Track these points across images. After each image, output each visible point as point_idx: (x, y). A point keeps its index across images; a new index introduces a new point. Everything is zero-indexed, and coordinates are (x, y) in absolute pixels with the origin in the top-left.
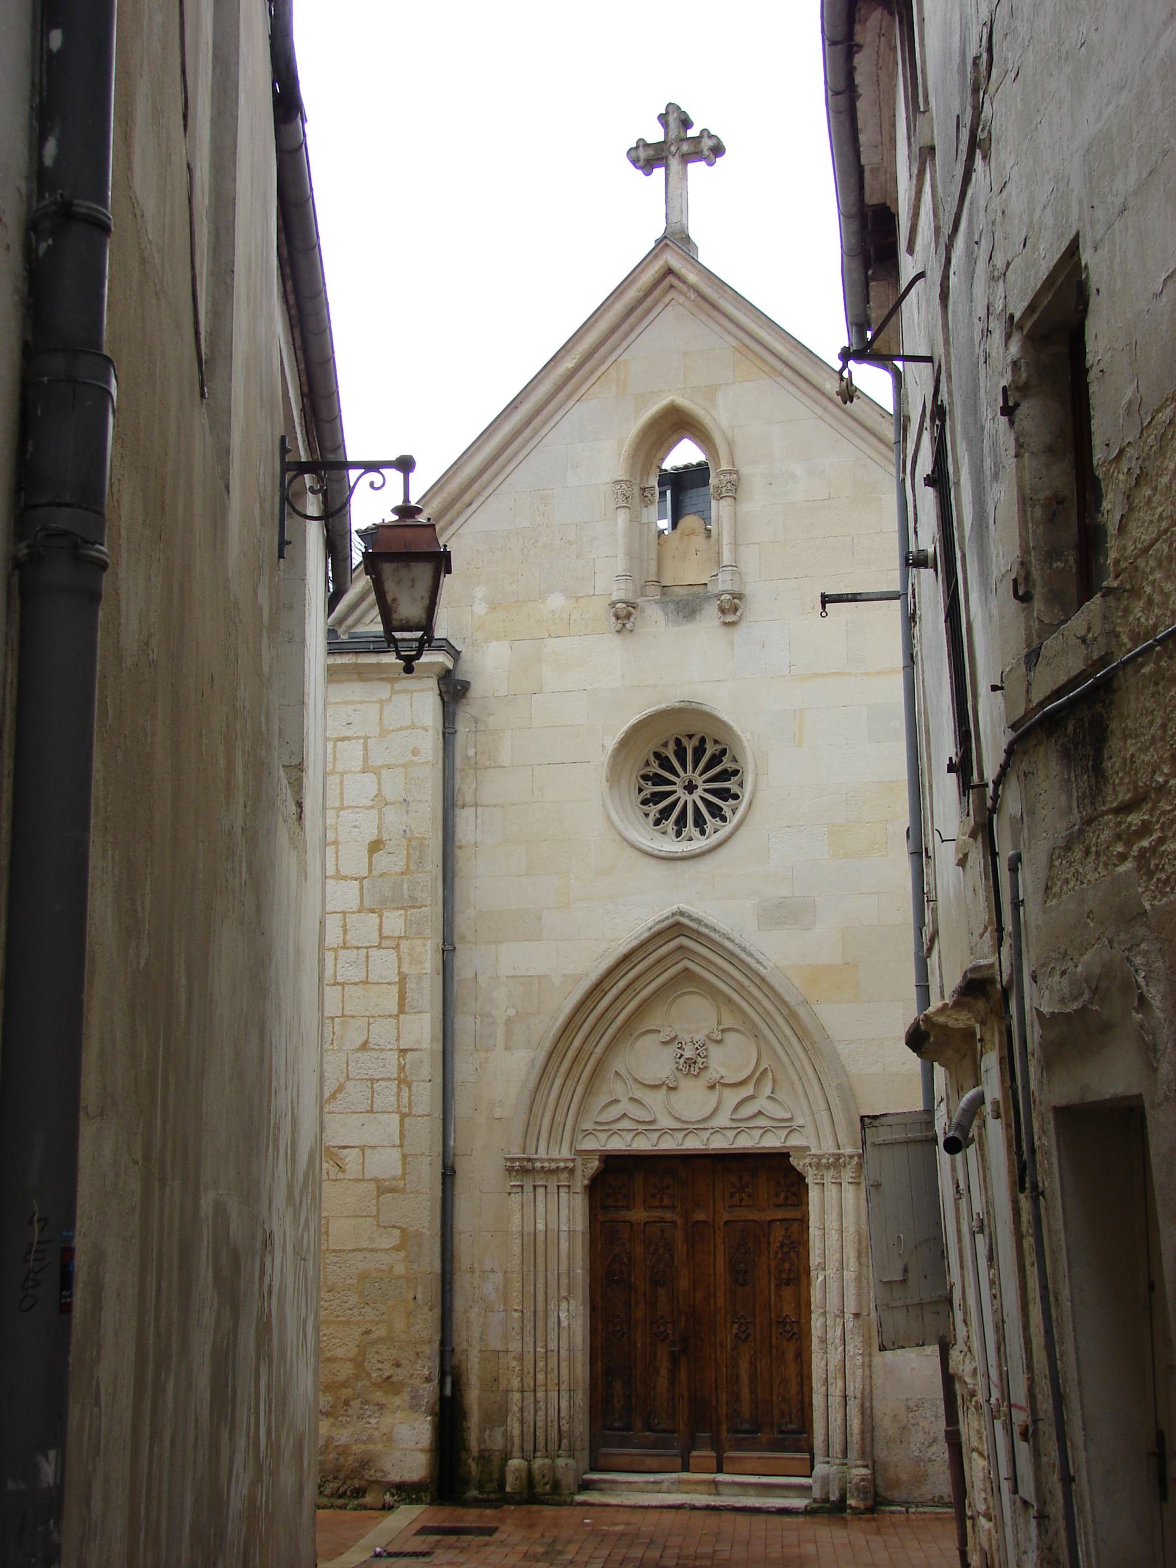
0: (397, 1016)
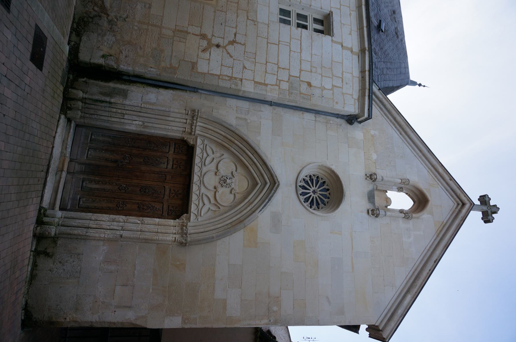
0: (254, 81)
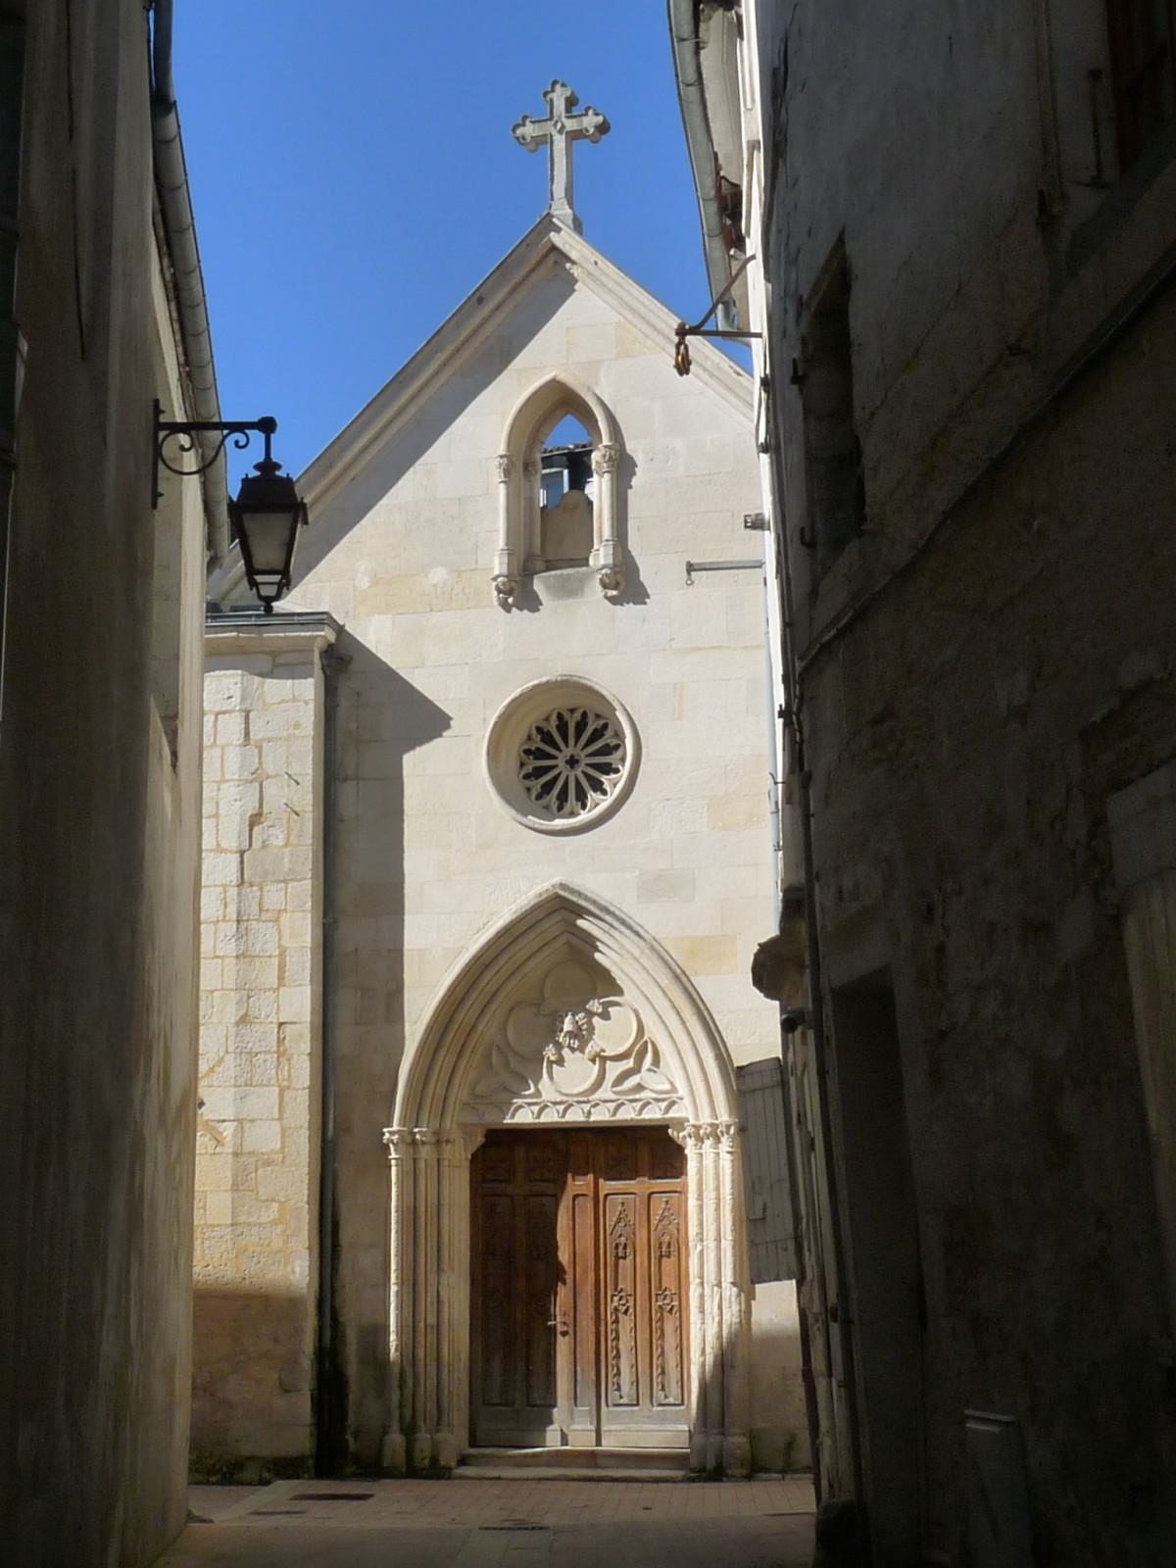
0: (278, 989)
